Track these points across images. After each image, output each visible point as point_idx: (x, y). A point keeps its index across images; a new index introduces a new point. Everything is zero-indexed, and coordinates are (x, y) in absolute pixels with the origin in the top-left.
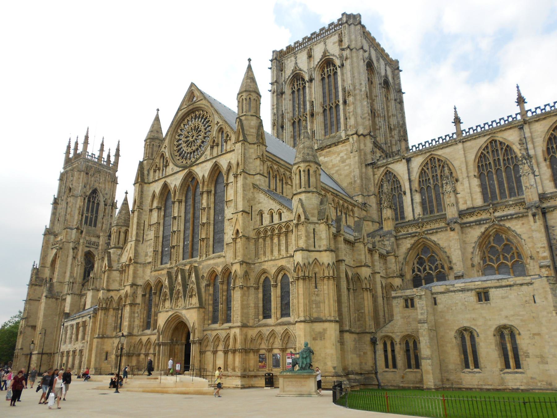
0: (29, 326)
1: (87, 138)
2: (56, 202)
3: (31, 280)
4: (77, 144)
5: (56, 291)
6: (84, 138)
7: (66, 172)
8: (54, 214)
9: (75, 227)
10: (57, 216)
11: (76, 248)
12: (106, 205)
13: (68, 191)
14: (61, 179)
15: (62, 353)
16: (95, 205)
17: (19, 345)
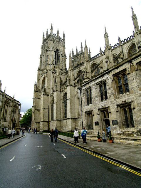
0: (36, 110)
1: (52, 27)
2: (41, 57)
3: (35, 90)
4: (47, 32)
5: (47, 92)
6: (51, 27)
7: (44, 45)
8: (41, 62)
9: (51, 64)
10: (42, 62)
11: (53, 72)
12: (62, 56)
13: (46, 52)
14: (42, 48)
15: (89, 114)
16: (58, 56)
17: (33, 118)
